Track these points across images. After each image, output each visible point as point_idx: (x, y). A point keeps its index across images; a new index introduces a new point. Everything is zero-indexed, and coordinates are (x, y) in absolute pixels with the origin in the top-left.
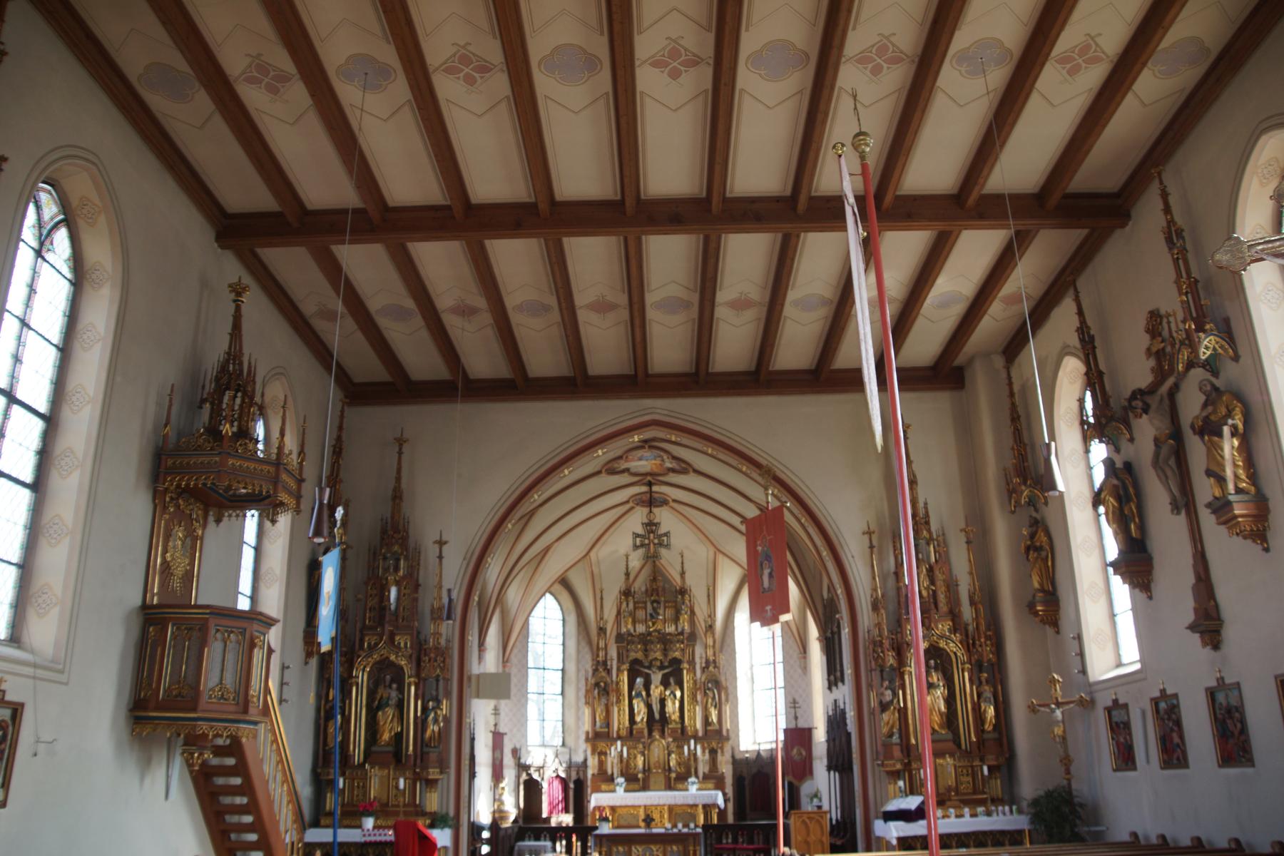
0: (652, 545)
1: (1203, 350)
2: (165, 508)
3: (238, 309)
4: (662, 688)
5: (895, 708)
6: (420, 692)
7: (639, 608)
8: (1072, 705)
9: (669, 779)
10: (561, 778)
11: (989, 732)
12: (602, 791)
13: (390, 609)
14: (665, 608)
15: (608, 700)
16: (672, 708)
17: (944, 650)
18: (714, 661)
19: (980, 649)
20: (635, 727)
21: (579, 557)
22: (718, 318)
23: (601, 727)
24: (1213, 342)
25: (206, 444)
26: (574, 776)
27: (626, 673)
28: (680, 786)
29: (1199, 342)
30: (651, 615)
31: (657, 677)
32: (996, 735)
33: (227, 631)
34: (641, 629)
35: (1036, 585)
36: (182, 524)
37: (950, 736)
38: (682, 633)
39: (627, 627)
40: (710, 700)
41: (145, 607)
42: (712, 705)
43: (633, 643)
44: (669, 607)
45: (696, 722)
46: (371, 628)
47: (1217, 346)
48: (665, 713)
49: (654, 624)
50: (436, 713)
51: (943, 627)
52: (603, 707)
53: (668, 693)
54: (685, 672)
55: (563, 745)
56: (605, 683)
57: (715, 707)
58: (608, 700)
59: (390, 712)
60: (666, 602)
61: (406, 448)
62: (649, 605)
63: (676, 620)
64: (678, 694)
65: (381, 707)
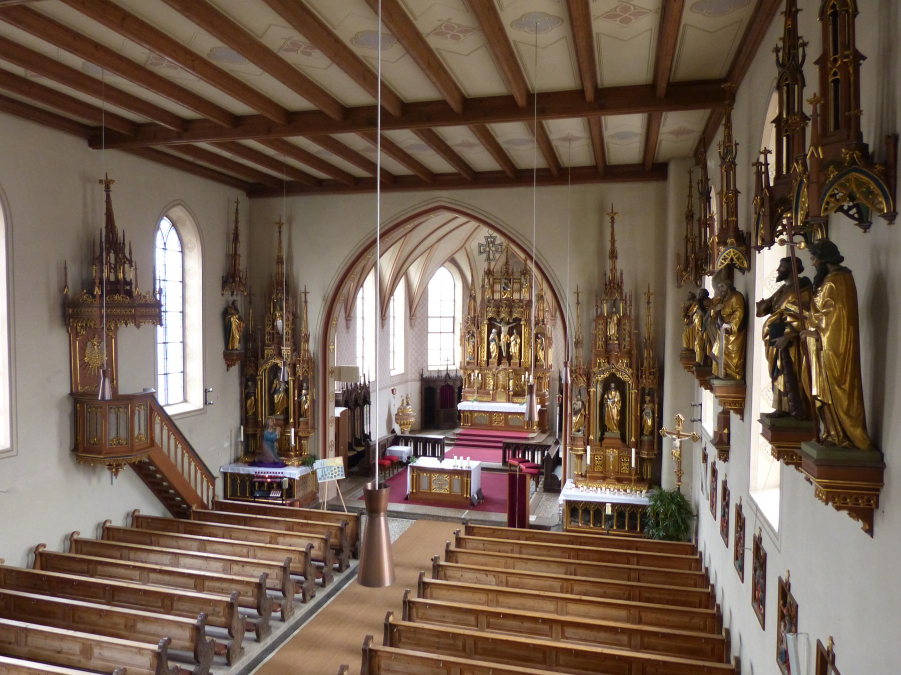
0: (491, 252)
1: (721, 260)
2: (77, 334)
3: (108, 197)
4: (508, 336)
5: (582, 414)
6: (296, 385)
7: (496, 282)
8: (687, 438)
9: (509, 395)
10: (450, 386)
11: (647, 435)
12: (467, 401)
13: (278, 333)
14: (514, 282)
15: (474, 342)
16: (514, 349)
17: (619, 378)
18: (543, 321)
19: (644, 381)
20: (490, 360)
21: (458, 248)
22: (598, 34)
23: (470, 359)
24: (732, 254)
25: (88, 299)
26: (458, 384)
27: (486, 326)
28: (515, 399)
29: (718, 254)
30: (504, 288)
31: (504, 329)
32: (651, 438)
33: (117, 407)
34: (497, 296)
35: (685, 346)
36: (96, 336)
37: (619, 436)
38: (521, 301)
39: (488, 295)
40: (539, 345)
41: (71, 394)
42: (540, 348)
43: (490, 307)
44: (516, 282)
45: (528, 357)
46: (269, 346)
47: (734, 258)
48: (510, 352)
49: (505, 294)
50: (306, 398)
51: (622, 364)
52: (471, 346)
53: (512, 339)
54: (523, 326)
55: (454, 364)
56: (473, 332)
57: (543, 350)
58: (474, 342)
59: (281, 395)
60: (514, 279)
61: (285, 229)
62: (503, 281)
63: (520, 291)
64: (519, 341)
65: (276, 391)
